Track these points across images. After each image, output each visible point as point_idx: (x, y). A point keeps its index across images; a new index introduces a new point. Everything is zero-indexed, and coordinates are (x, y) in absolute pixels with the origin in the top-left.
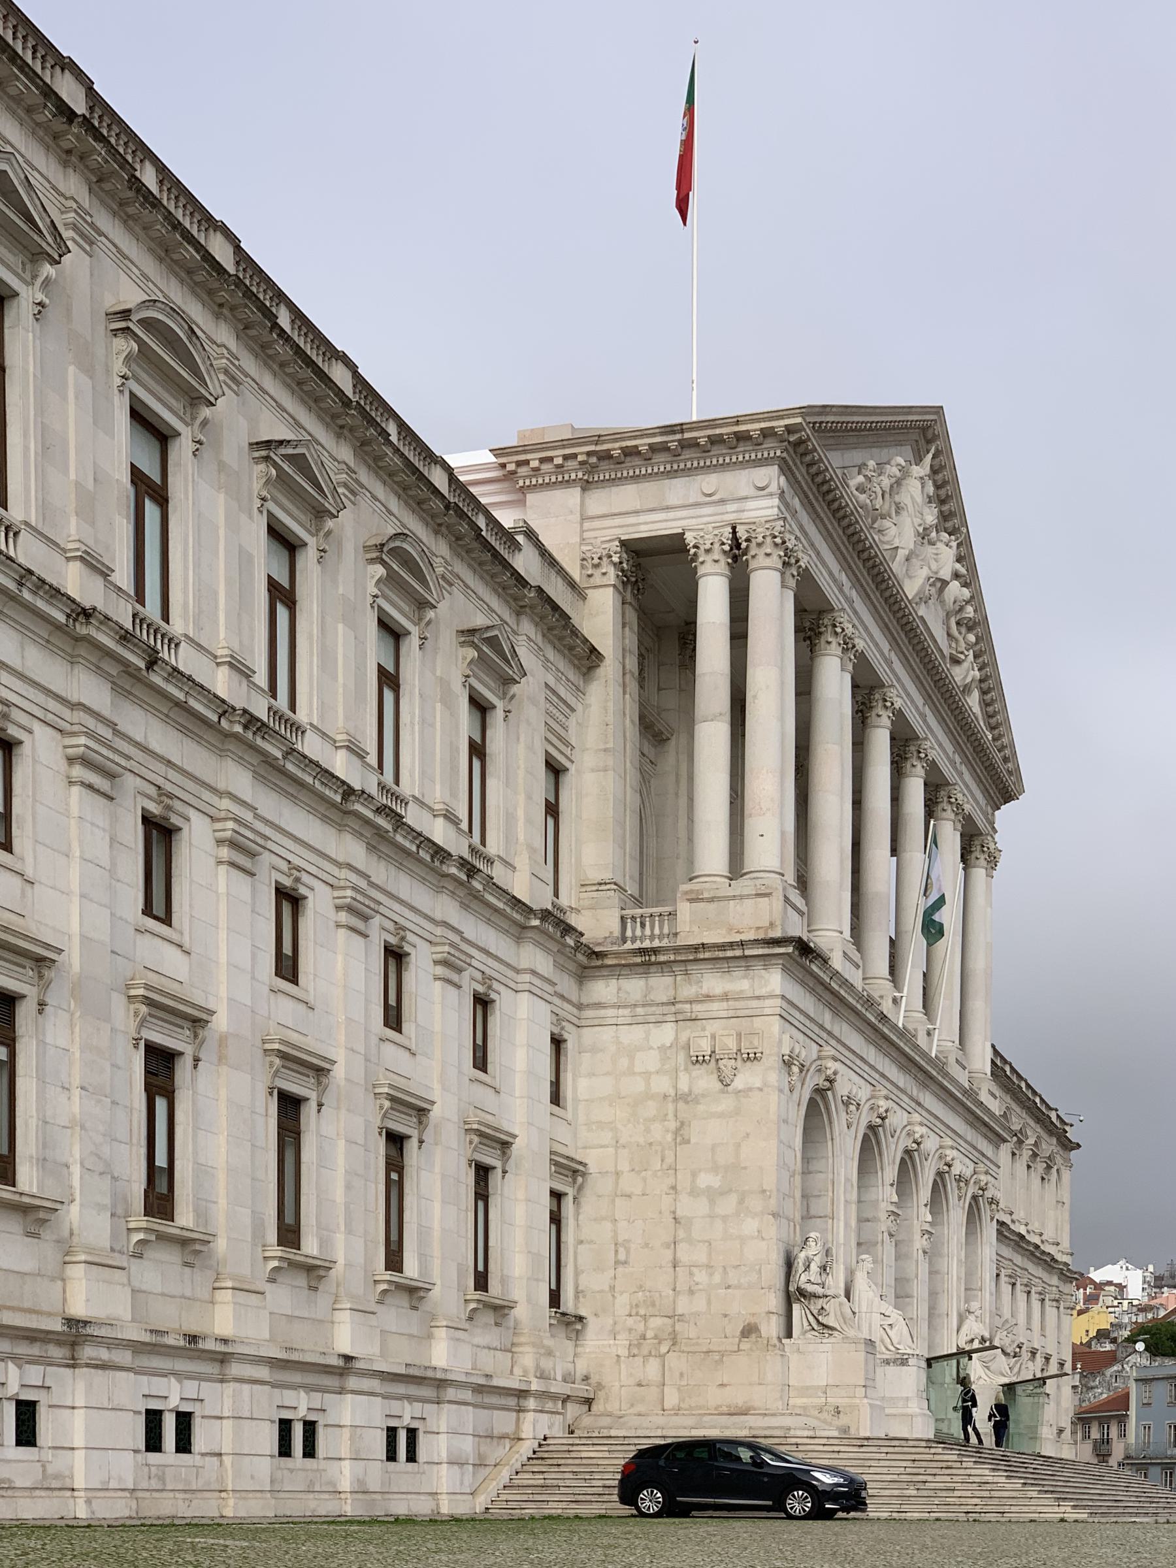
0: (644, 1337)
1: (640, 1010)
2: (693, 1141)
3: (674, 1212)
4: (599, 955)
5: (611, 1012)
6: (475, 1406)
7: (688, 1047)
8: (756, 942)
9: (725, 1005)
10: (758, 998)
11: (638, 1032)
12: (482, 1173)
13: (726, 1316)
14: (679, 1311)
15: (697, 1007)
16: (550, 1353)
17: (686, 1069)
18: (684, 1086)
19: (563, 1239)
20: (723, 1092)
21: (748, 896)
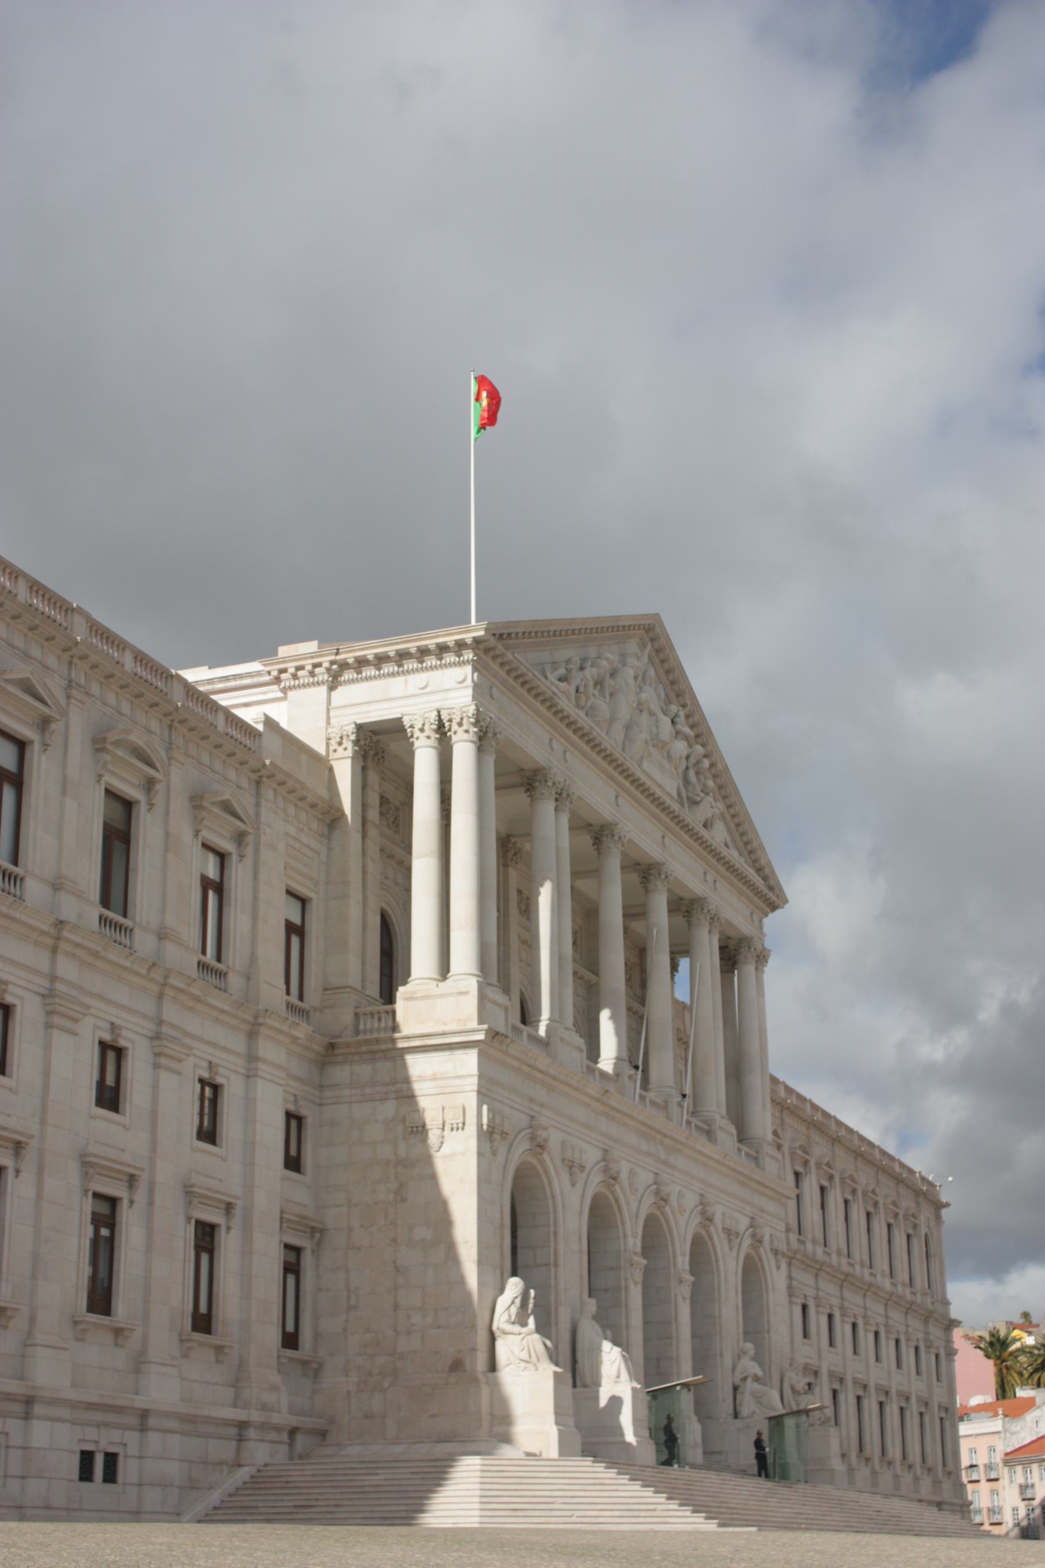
0: (370, 1374)
1: (368, 1090)
6: (182, 1434)
7: (404, 1120)
9: (433, 1084)
10: (460, 1077)
13: (437, 1353)
16: (274, 1388)
17: (404, 1138)
18: (402, 1152)
19: (302, 1288)
21: (451, 994)
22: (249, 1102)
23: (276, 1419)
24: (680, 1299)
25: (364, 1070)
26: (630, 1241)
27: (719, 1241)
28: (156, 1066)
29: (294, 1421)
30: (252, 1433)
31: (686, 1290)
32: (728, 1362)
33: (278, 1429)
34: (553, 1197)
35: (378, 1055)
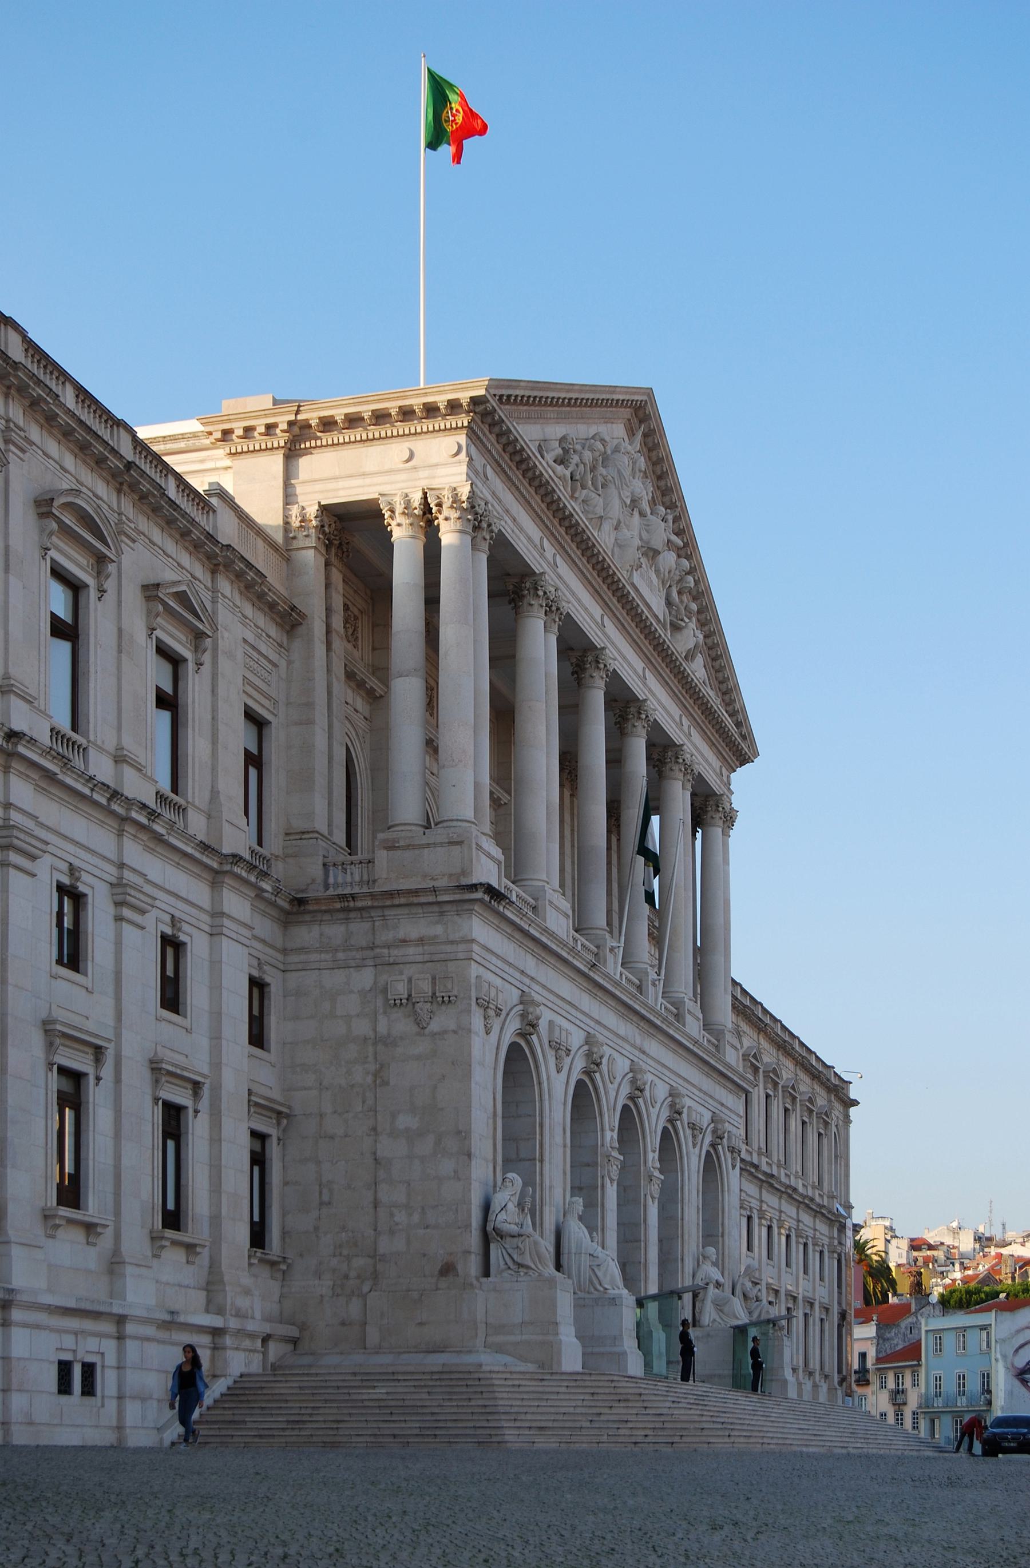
0: (346, 1277)
1: (341, 955)
2: (392, 1083)
3: (375, 1153)
4: (301, 902)
5: (314, 957)
6: (158, 1341)
7: (385, 991)
8: (447, 890)
9: (420, 949)
10: (452, 942)
11: (338, 978)
12: (173, 1112)
13: (424, 1255)
14: (381, 1250)
15: (395, 952)
16: (247, 1292)
17: (385, 1013)
18: (382, 1028)
20: (418, 1034)
21: (441, 844)
22: (215, 965)
23: (251, 1326)
24: (649, 1197)
25: (335, 931)
26: (608, 1134)
27: (685, 1134)
28: (119, 919)
29: (267, 1328)
30: (228, 1341)
31: (655, 1189)
32: (689, 1265)
33: (252, 1336)
34: (540, 1084)
35: (352, 915)
